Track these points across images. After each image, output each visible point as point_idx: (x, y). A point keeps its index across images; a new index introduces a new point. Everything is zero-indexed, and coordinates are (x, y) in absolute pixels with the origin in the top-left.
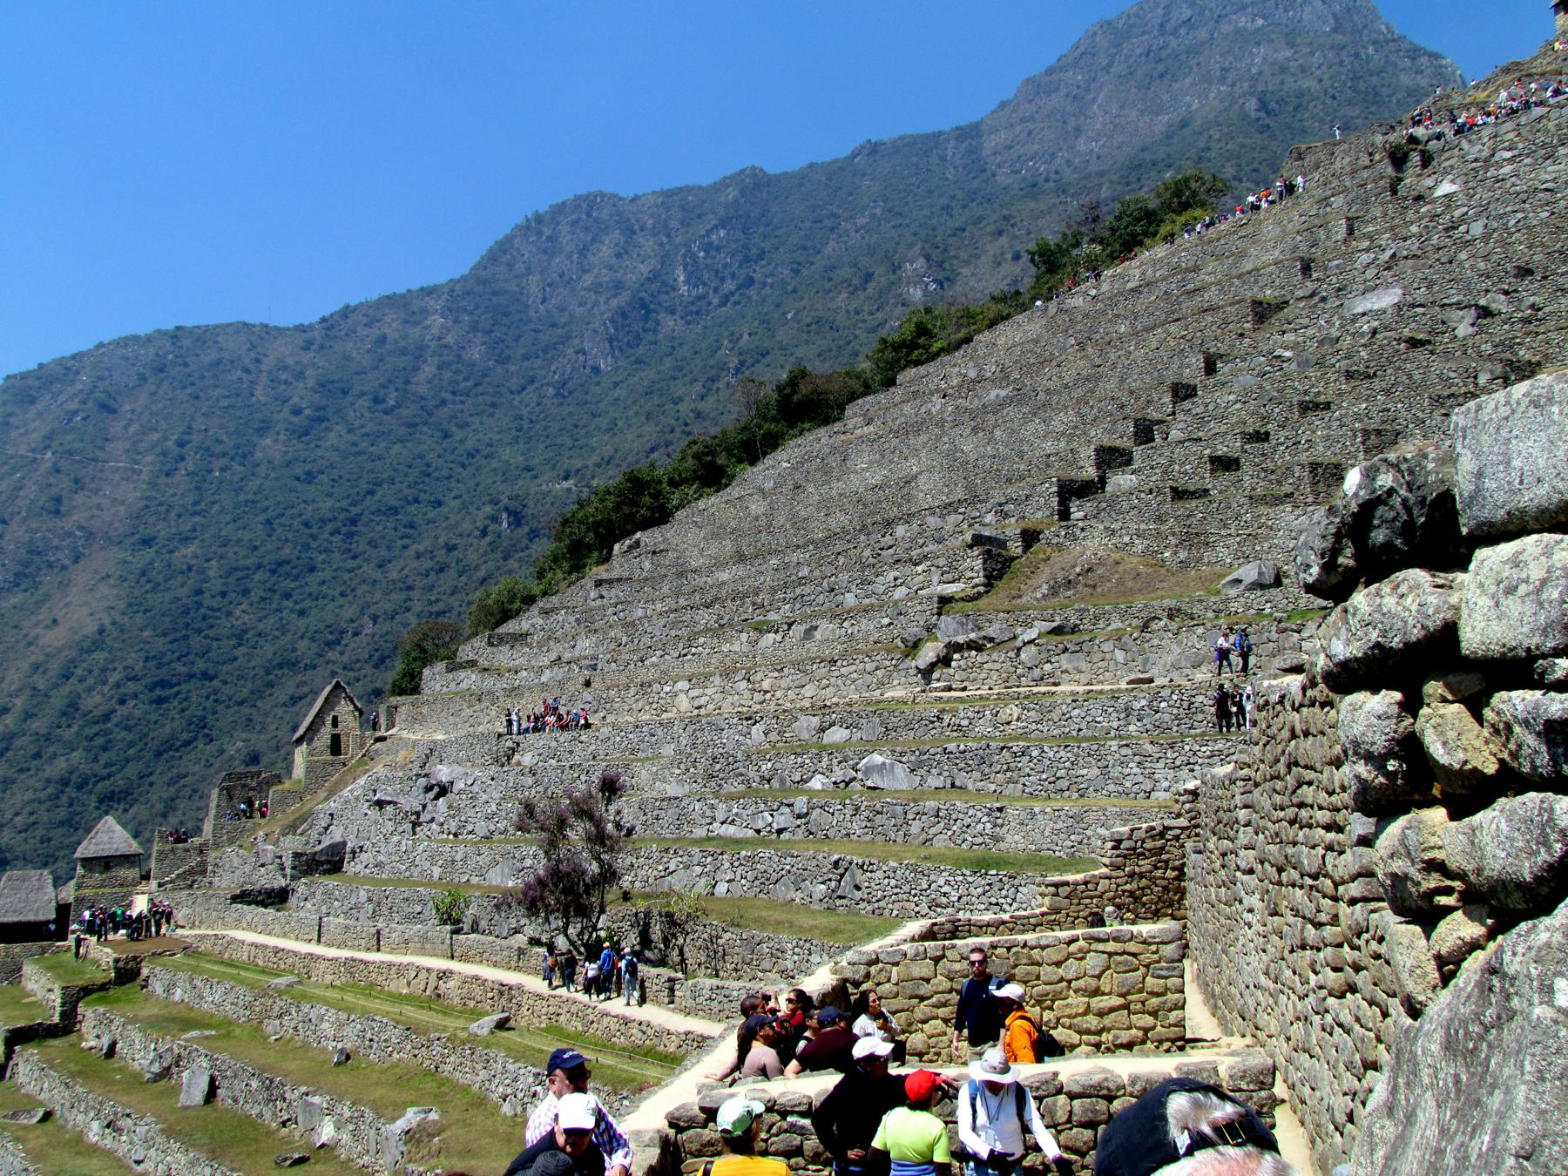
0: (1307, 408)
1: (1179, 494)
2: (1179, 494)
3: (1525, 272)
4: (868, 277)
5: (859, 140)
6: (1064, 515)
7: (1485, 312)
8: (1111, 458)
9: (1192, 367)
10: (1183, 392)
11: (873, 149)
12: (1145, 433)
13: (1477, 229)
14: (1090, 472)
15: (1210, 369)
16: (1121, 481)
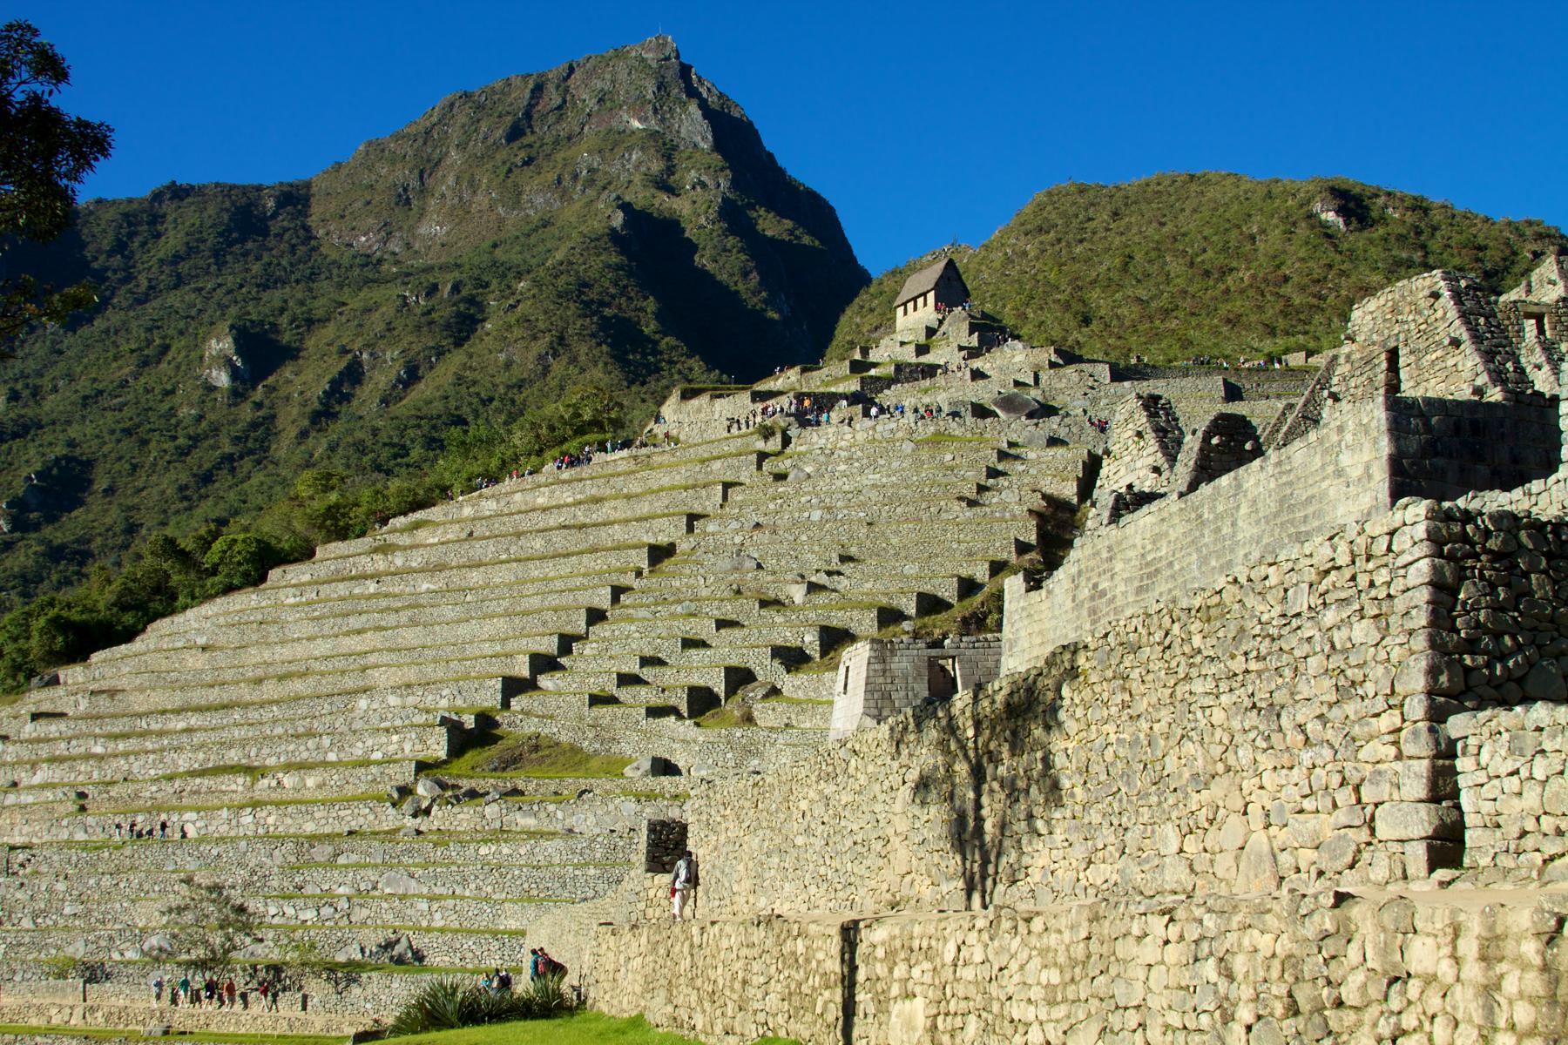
0: (689, 643)
1: (595, 700)
2: (595, 700)
3: (845, 559)
4: (165, 349)
5: (166, 182)
6: (506, 705)
7: (813, 588)
8: (543, 664)
9: (602, 599)
10: (596, 616)
11: (178, 193)
12: (566, 643)
13: (816, 515)
14: (525, 672)
15: (615, 599)
16: (545, 681)
